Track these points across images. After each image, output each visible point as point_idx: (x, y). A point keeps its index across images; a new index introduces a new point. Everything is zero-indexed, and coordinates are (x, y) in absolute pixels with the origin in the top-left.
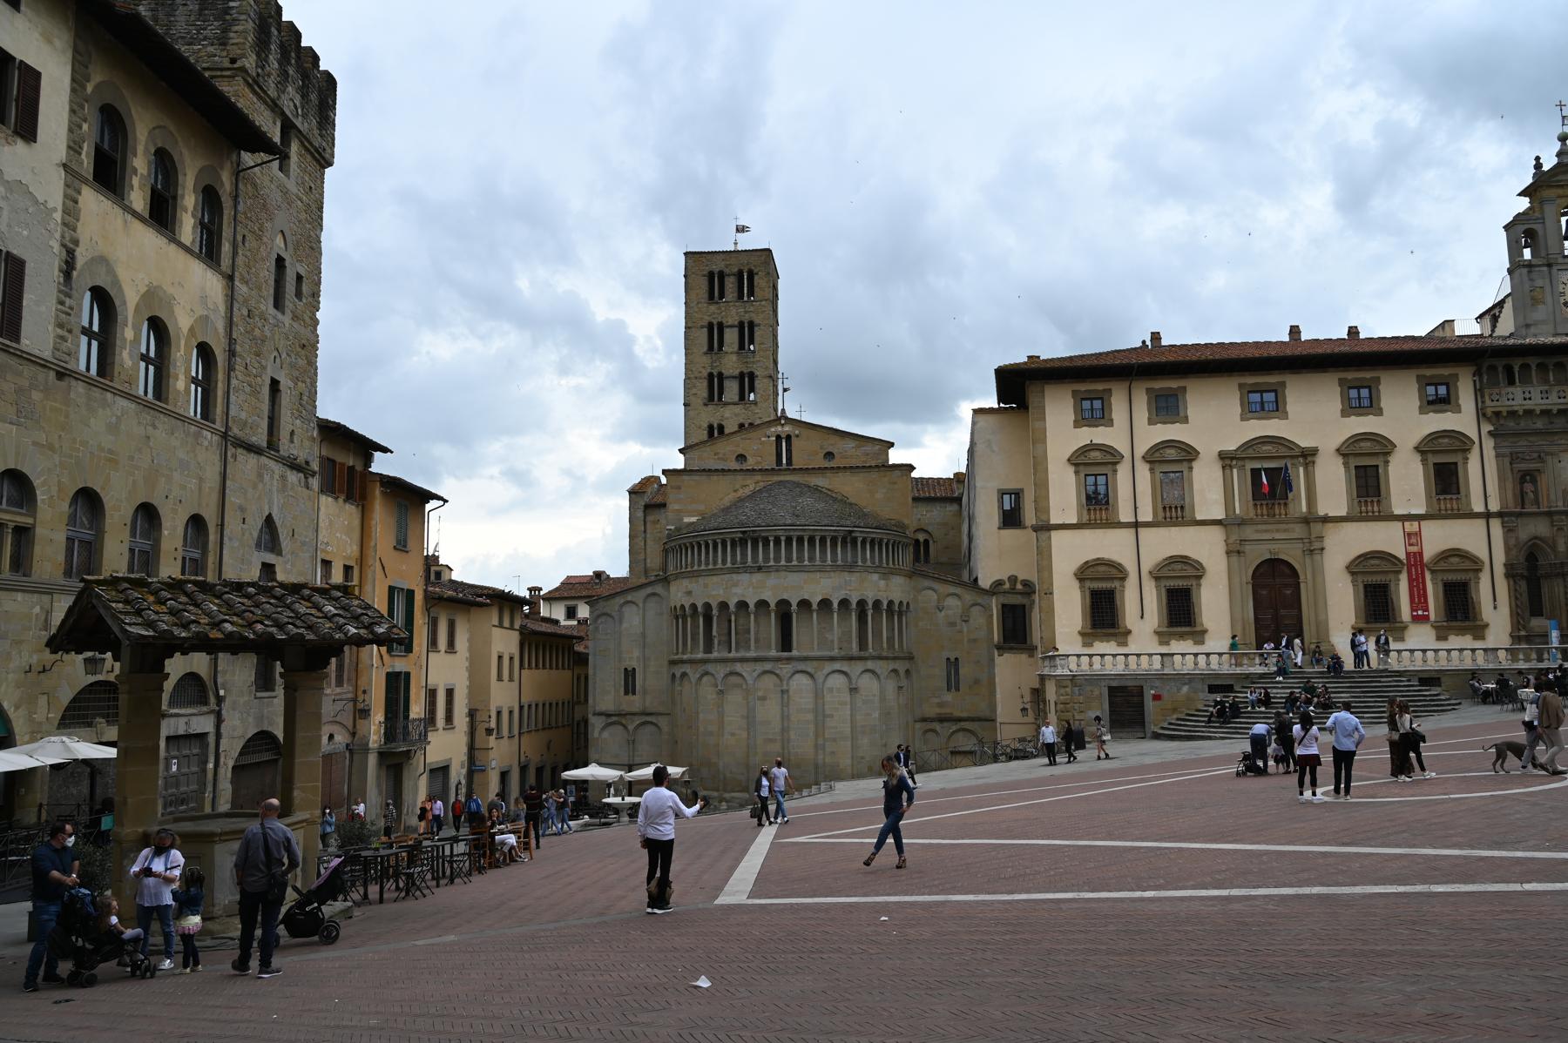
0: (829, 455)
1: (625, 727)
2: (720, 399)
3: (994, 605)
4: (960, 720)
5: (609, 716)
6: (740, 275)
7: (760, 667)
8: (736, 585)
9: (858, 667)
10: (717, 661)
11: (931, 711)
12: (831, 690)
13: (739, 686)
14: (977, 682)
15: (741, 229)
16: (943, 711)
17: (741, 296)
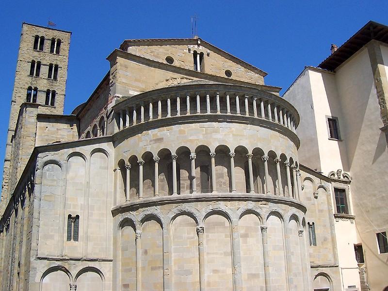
0: (228, 73)
1: (67, 271)
3: (331, 187)
7: (245, 206)
8: (216, 131)
10: (198, 200)
13: (222, 224)
14: (325, 240)
17: (52, 51)
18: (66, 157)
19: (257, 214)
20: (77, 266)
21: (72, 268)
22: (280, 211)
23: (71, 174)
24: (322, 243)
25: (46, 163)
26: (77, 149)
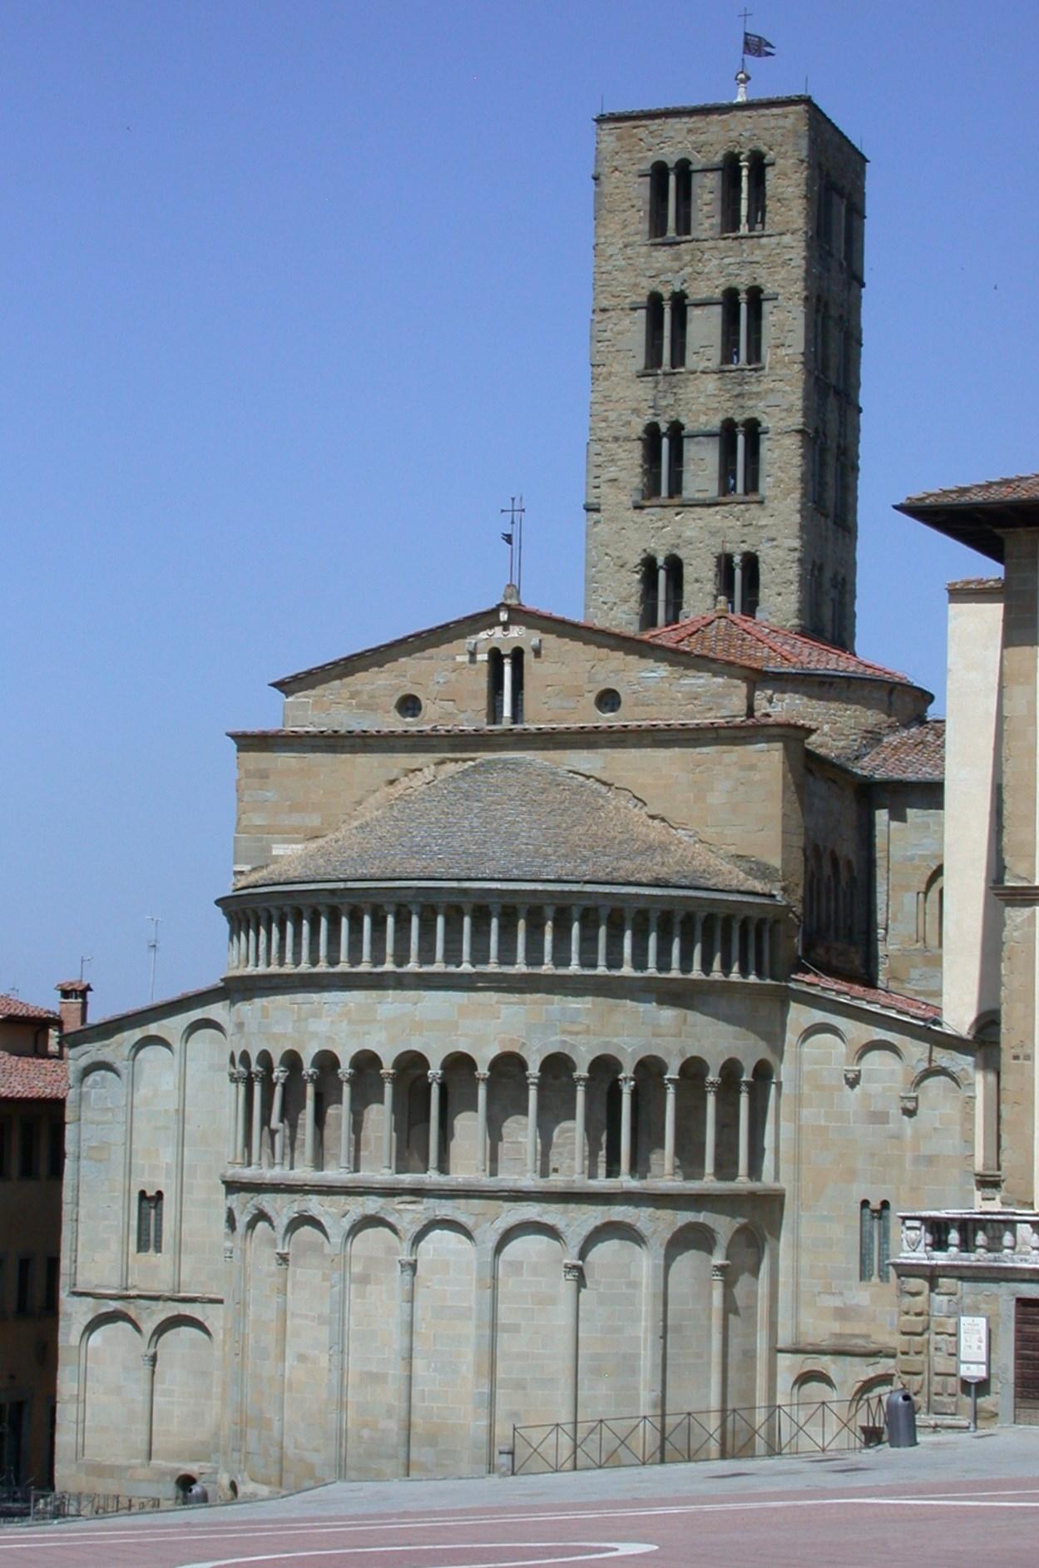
0: (608, 700)
2: (676, 487)
6: (730, 168)
8: (316, 1014)
12: (516, 1267)
13: (317, 1249)
15: (755, 46)
16: (850, 1328)
17: (730, 222)
18: (126, 1050)
20: (153, 1312)
21: (144, 1315)
22: (462, 1218)
23: (142, 1092)
25: (87, 1071)
26: (153, 1029)
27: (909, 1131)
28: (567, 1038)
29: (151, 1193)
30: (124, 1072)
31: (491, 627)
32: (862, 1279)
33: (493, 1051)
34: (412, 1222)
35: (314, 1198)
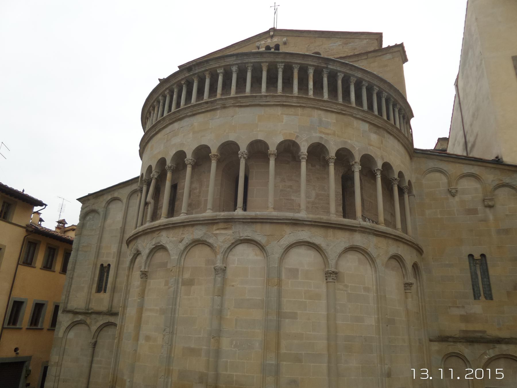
4: (499, 341)
5: (75, 313)
9: (342, 240)
11: (455, 327)
12: (294, 272)
19: (210, 245)
22: (258, 238)
23: (109, 221)
24: (508, 293)
26: (116, 195)
27: (491, 217)
28: (323, 136)
29: (105, 265)
30: (102, 213)
31: (267, 38)
32: (475, 299)
33: (280, 139)
34: (223, 242)
35: (164, 234)
